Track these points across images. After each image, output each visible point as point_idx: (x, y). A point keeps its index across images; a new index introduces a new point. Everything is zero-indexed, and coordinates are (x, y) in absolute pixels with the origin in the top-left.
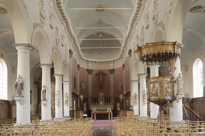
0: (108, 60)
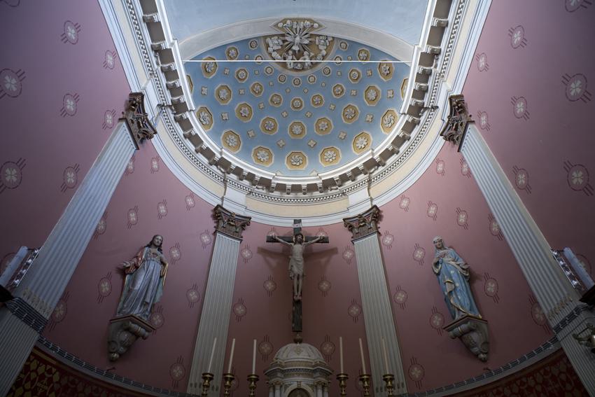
0: (334, 174)
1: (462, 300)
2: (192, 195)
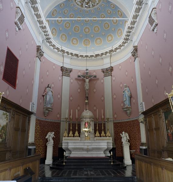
1: (127, 103)
2: (54, 64)
